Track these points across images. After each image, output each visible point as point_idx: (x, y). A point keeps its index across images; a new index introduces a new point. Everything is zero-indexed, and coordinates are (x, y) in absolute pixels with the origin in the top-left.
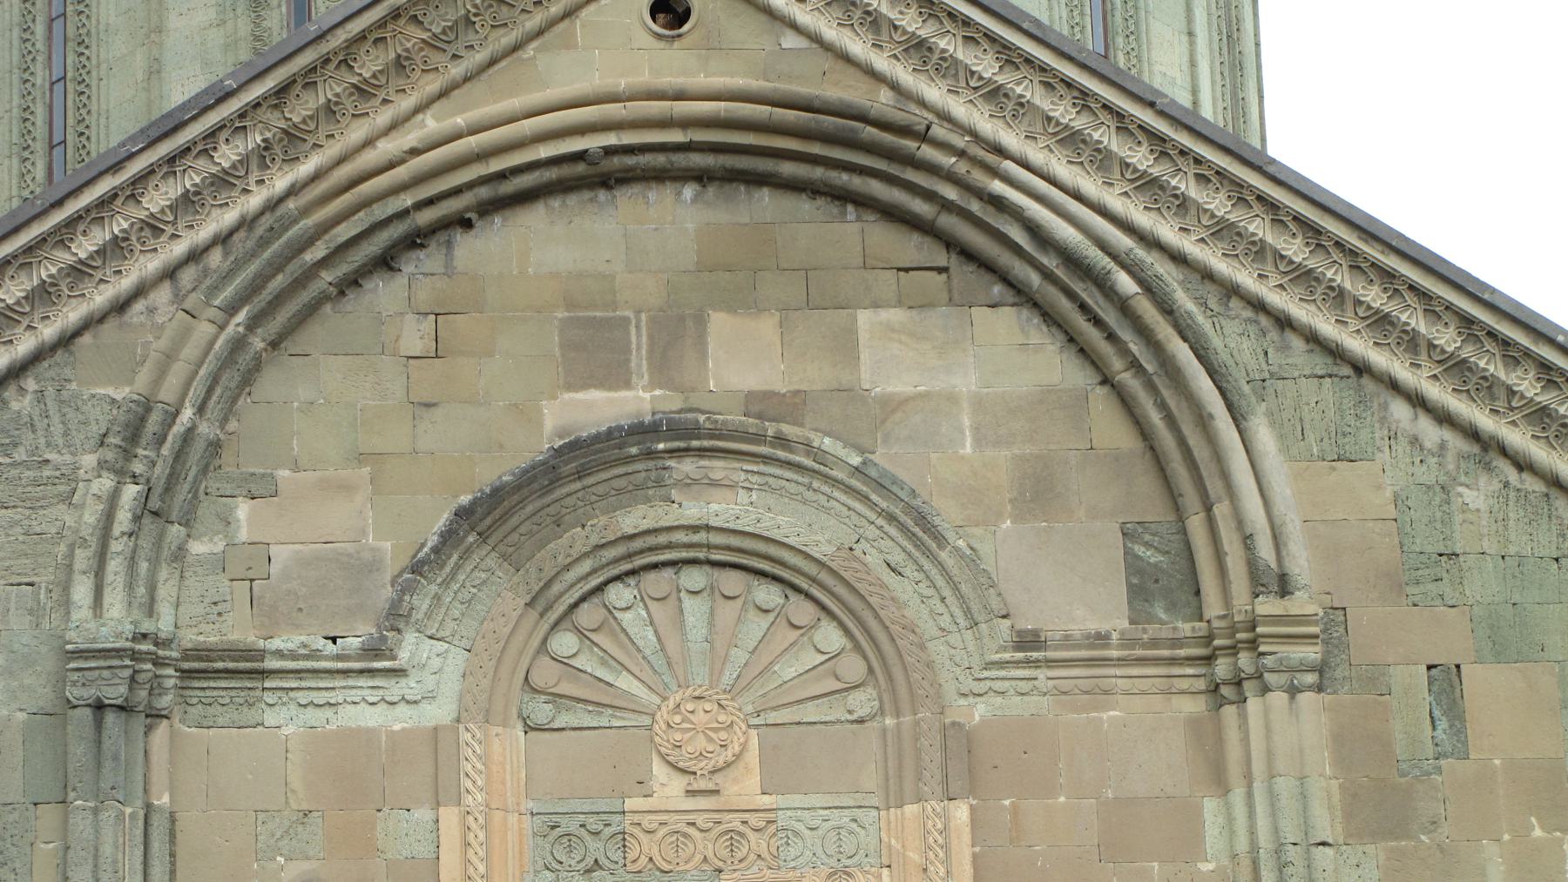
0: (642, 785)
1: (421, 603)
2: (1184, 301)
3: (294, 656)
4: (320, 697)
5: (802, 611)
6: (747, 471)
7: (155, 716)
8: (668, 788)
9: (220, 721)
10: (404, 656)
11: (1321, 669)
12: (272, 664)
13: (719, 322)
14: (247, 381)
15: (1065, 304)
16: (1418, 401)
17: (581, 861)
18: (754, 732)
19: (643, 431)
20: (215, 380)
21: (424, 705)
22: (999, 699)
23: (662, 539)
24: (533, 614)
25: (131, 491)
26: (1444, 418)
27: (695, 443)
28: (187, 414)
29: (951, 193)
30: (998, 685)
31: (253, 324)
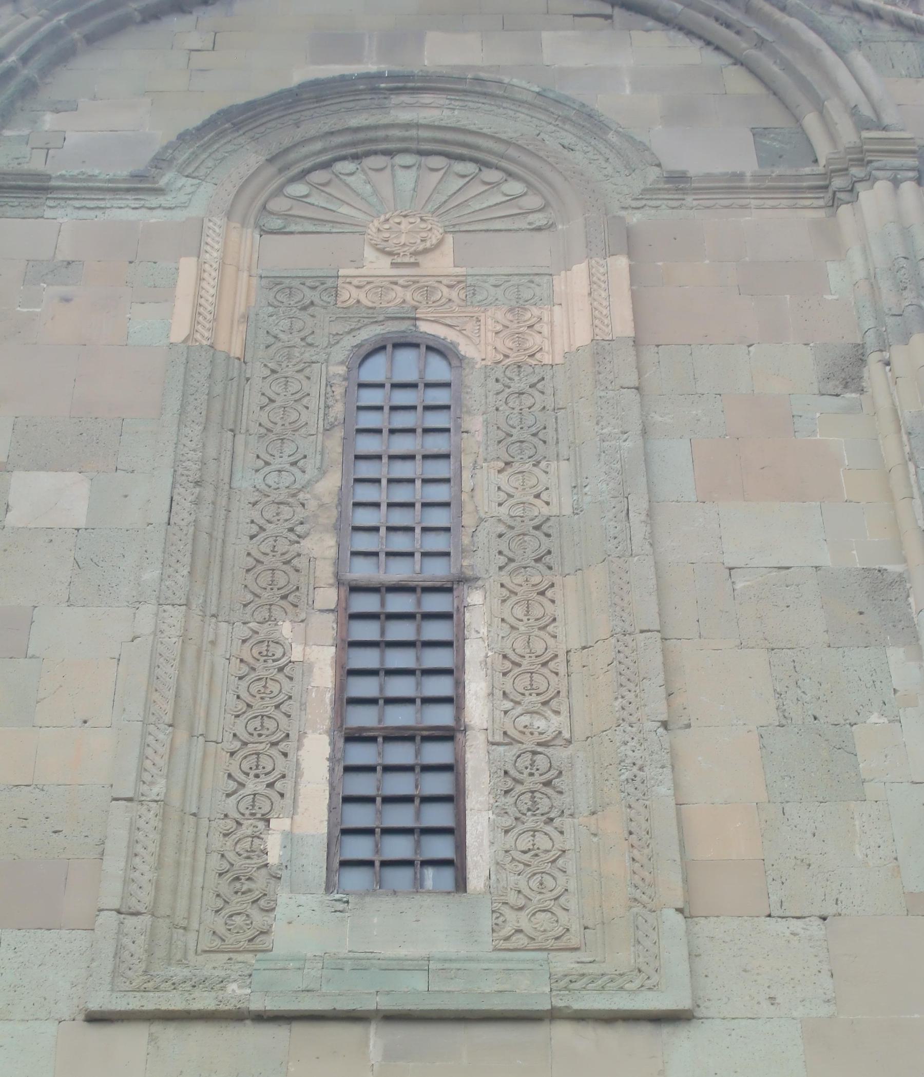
0: (357, 262)
1: (182, 157)
3: (73, 178)
6: (451, 99)
8: (377, 265)
9: (8, 214)
10: (162, 183)
12: (53, 183)
17: (300, 302)
18: (450, 238)
20: (34, 50)
22: (653, 211)
23: (381, 134)
24: (271, 170)
27: (410, 85)
28: (12, 58)
31: (72, 23)
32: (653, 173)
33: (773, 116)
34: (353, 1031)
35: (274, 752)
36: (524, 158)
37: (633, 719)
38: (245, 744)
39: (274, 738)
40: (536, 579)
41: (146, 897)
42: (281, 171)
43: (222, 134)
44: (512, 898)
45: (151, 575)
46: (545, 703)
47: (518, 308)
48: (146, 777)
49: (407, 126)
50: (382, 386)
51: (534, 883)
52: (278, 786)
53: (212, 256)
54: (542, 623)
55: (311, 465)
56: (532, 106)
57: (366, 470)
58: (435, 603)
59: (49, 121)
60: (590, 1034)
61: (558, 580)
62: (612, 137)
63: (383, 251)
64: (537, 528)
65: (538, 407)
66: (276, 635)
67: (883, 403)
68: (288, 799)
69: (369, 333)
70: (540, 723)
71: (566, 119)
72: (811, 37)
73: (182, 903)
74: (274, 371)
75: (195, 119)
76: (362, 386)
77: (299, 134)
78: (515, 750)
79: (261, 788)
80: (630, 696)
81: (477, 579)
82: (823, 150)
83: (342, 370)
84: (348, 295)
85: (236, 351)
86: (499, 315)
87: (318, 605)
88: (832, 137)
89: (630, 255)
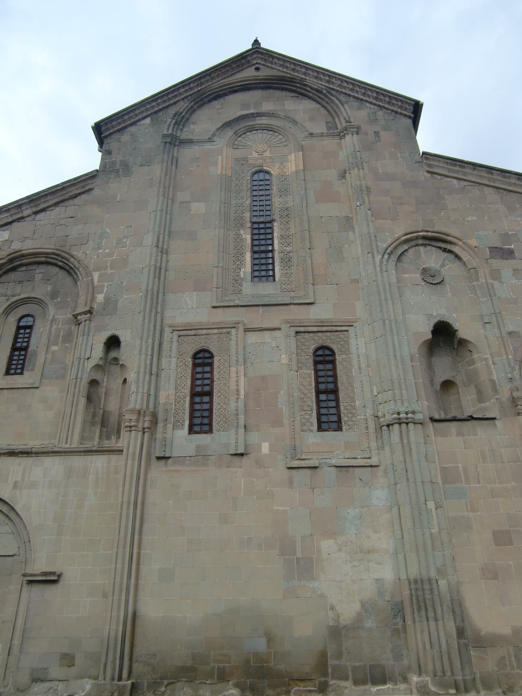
0: (251, 154)
1: (218, 133)
3: (198, 140)
4: (201, 145)
7: (175, 146)
8: (255, 155)
10: (214, 139)
12: (194, 141)
13: (264, 103)
15: (316, 97)
16: (371, 103)
18: (269, 148)
19: (252, 114)
20: (188, 111)
21: (217, 146)
23: (255, 126)
24: (235, 135)
25: (174, 121)
28: (184, 113)
30: (307, 140)
31: (195, 104)
32: (307, 133)
33: (330, 119)
34: (257, 308)
35: (241, 256)
36: (282, 131)
37: (304, 248)
38: (236, 255)
39: (241, 254)
40: (286, 220)
41: (221, 285)
42: (236, 135)
43: (225, 128)
44: (283, 282)
45: (217, 223)
46: (288, 245)
47: (282, 163)
48: (219, 262)
49: (260, 124)
50: (257, 181)
51: (287, 279)
52: (242, 262)
53: (224, 155)
54: (287, 229)
55: (245, 198)
56: (284, 119)
57: (255, 198)
58: (268, 225)
59: (192, 126)
60: (297, 307)
61: (290, 220)
62: (299, 125)
63: (256, 152)
64: (286, 209)
65: (286, 184)
66: (240, 233)
67: (349, 182)
68: (244, 265)
69: (254, 169)
70: (287, 249)
71: (290, 122)
72: (337, 102)
73: (227, 286)
74: (237, 179)
75: (219, 125)
76: (253, 181)
77: (239, 127)
78: (283, 254)
79: (239, 263)
80: (303, 243)
81: (275, 220)
82: (339, 127)
83: (249, 178)
84: (250, 161)
85: (230, 175)
86: (278, 165)
87: (247, 227)
88: (341, 124)
89: (302, 151)
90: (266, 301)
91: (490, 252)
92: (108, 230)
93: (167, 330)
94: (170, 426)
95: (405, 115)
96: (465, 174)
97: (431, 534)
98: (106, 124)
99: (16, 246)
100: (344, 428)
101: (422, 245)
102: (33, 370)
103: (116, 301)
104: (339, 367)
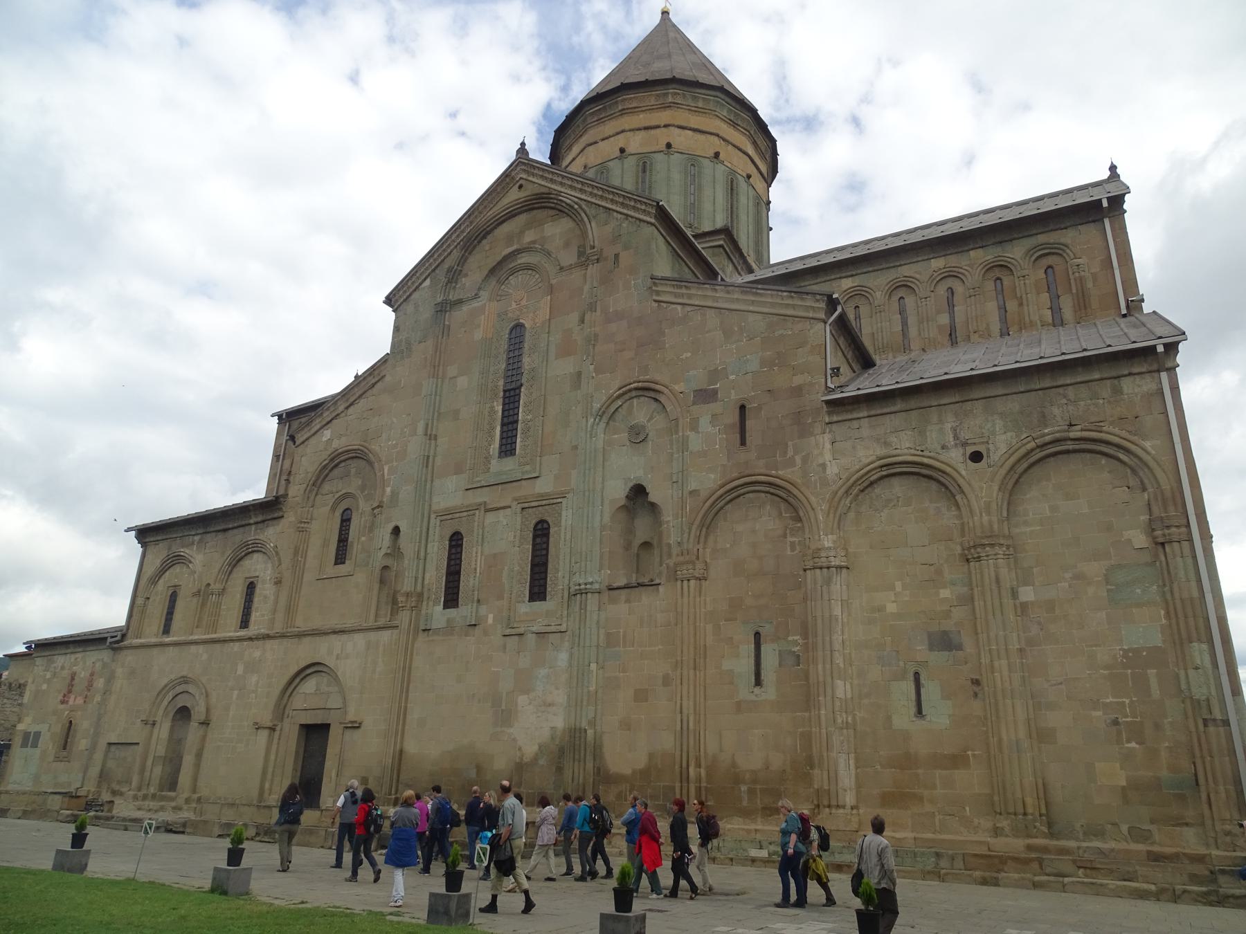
2: (584, 206)
5: (534, 273)
7: (446, 311)
8: (514, 305)
11: (598, 259)
14: (465, 261)
26: (621, 213)
29: (555, 201)
31: (465, 252)
83: (507, 336)
90: (504, 478)
91: (694, 396)
92: (395, 420)
93: (433, 516)
94: (431, 603)
95: (648, 223)
96: (690, 296)
97: (589, 692)
98: (395, 295)
99: (336, 444)
100: (547, 598)
101: (636, 397)
102: (351, 559)
103: (398, 493)
104: (551, 539)
